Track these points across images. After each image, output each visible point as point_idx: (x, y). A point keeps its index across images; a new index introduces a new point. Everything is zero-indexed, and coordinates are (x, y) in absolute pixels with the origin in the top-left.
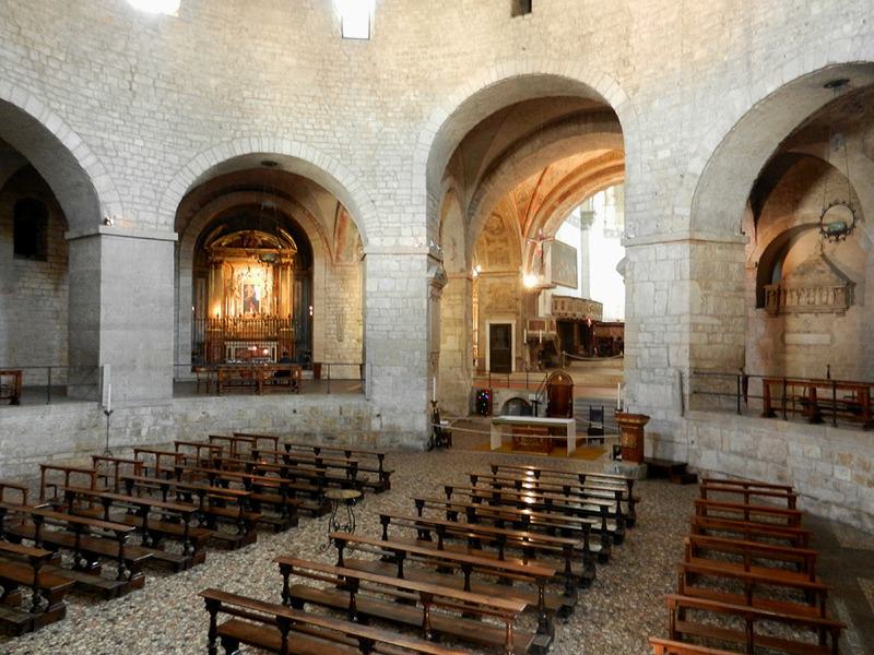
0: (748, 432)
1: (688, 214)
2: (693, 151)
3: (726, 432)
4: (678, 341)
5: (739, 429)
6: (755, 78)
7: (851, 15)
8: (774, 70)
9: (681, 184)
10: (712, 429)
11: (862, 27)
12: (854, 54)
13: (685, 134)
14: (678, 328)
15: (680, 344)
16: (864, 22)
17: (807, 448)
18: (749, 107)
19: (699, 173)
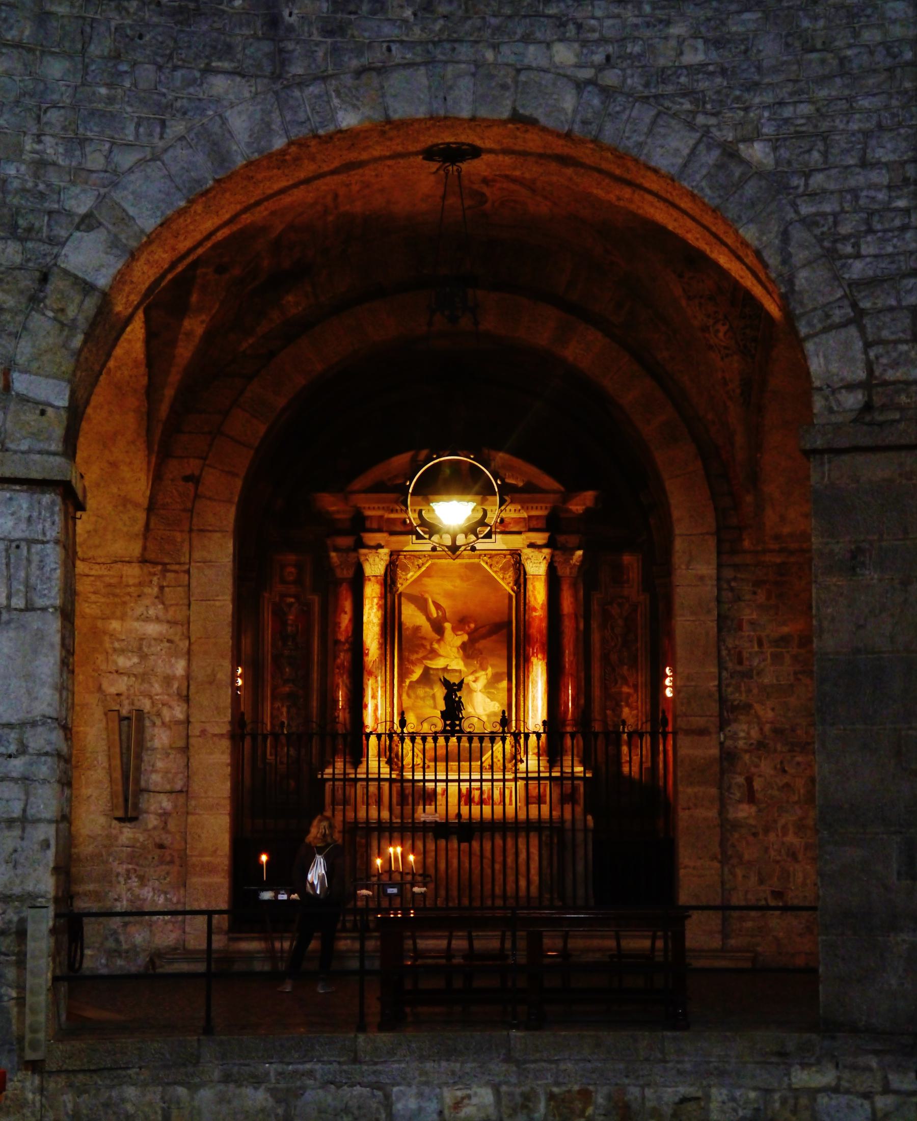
0: (257, 1081)
1: (63, 402)
2: (82, 210)
3: (182, 1091)
4: (16, 810)
5: (227, 1079)
6: (297, 69)
7: (571, 30)
8: (359, 73)
9: (35, 300)
10: (131, 1092)
11: (600, 69)
12: (585, 122)
13: (51, 148)
14: (17, 765)
15: (24, 821)
16: (608, 58)
17: (449, 1095)
18: (279, 143)
19: (102, 281)
